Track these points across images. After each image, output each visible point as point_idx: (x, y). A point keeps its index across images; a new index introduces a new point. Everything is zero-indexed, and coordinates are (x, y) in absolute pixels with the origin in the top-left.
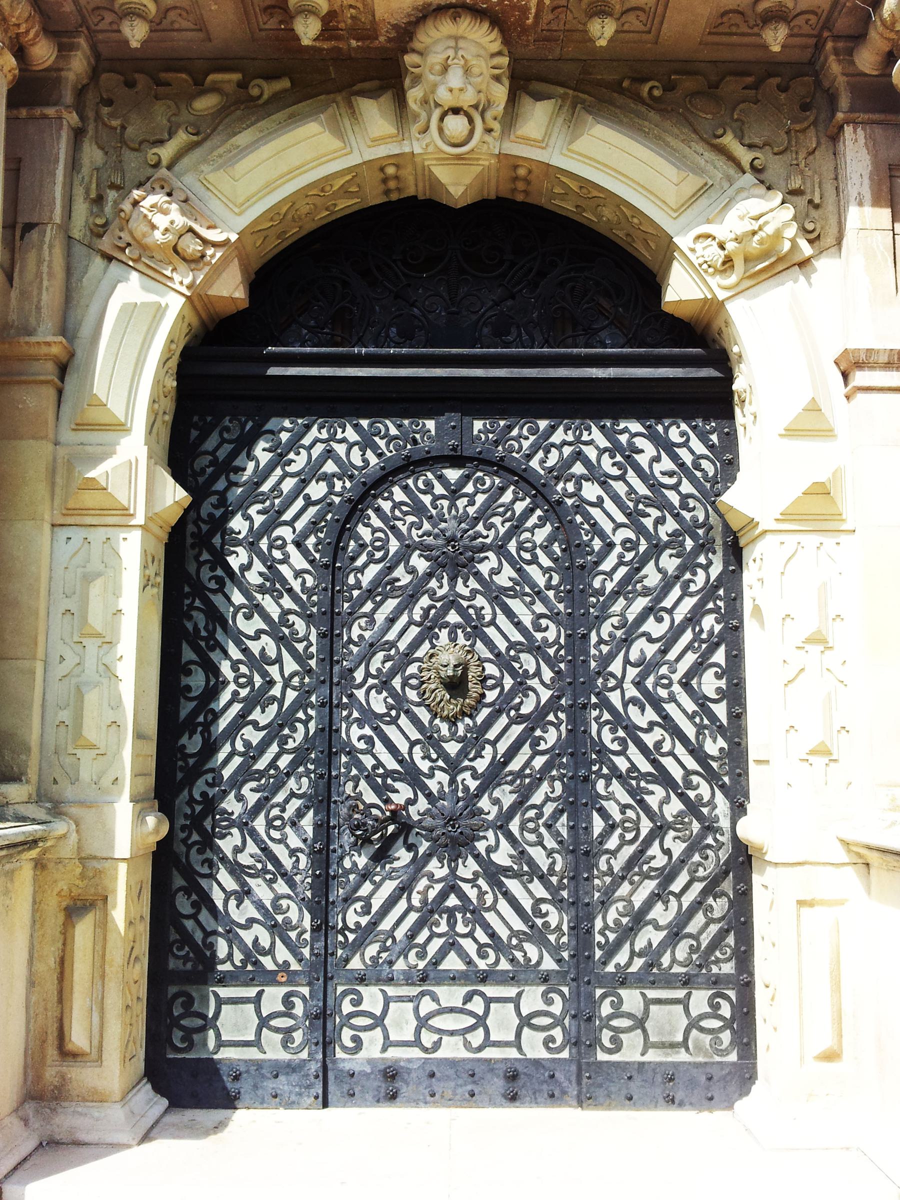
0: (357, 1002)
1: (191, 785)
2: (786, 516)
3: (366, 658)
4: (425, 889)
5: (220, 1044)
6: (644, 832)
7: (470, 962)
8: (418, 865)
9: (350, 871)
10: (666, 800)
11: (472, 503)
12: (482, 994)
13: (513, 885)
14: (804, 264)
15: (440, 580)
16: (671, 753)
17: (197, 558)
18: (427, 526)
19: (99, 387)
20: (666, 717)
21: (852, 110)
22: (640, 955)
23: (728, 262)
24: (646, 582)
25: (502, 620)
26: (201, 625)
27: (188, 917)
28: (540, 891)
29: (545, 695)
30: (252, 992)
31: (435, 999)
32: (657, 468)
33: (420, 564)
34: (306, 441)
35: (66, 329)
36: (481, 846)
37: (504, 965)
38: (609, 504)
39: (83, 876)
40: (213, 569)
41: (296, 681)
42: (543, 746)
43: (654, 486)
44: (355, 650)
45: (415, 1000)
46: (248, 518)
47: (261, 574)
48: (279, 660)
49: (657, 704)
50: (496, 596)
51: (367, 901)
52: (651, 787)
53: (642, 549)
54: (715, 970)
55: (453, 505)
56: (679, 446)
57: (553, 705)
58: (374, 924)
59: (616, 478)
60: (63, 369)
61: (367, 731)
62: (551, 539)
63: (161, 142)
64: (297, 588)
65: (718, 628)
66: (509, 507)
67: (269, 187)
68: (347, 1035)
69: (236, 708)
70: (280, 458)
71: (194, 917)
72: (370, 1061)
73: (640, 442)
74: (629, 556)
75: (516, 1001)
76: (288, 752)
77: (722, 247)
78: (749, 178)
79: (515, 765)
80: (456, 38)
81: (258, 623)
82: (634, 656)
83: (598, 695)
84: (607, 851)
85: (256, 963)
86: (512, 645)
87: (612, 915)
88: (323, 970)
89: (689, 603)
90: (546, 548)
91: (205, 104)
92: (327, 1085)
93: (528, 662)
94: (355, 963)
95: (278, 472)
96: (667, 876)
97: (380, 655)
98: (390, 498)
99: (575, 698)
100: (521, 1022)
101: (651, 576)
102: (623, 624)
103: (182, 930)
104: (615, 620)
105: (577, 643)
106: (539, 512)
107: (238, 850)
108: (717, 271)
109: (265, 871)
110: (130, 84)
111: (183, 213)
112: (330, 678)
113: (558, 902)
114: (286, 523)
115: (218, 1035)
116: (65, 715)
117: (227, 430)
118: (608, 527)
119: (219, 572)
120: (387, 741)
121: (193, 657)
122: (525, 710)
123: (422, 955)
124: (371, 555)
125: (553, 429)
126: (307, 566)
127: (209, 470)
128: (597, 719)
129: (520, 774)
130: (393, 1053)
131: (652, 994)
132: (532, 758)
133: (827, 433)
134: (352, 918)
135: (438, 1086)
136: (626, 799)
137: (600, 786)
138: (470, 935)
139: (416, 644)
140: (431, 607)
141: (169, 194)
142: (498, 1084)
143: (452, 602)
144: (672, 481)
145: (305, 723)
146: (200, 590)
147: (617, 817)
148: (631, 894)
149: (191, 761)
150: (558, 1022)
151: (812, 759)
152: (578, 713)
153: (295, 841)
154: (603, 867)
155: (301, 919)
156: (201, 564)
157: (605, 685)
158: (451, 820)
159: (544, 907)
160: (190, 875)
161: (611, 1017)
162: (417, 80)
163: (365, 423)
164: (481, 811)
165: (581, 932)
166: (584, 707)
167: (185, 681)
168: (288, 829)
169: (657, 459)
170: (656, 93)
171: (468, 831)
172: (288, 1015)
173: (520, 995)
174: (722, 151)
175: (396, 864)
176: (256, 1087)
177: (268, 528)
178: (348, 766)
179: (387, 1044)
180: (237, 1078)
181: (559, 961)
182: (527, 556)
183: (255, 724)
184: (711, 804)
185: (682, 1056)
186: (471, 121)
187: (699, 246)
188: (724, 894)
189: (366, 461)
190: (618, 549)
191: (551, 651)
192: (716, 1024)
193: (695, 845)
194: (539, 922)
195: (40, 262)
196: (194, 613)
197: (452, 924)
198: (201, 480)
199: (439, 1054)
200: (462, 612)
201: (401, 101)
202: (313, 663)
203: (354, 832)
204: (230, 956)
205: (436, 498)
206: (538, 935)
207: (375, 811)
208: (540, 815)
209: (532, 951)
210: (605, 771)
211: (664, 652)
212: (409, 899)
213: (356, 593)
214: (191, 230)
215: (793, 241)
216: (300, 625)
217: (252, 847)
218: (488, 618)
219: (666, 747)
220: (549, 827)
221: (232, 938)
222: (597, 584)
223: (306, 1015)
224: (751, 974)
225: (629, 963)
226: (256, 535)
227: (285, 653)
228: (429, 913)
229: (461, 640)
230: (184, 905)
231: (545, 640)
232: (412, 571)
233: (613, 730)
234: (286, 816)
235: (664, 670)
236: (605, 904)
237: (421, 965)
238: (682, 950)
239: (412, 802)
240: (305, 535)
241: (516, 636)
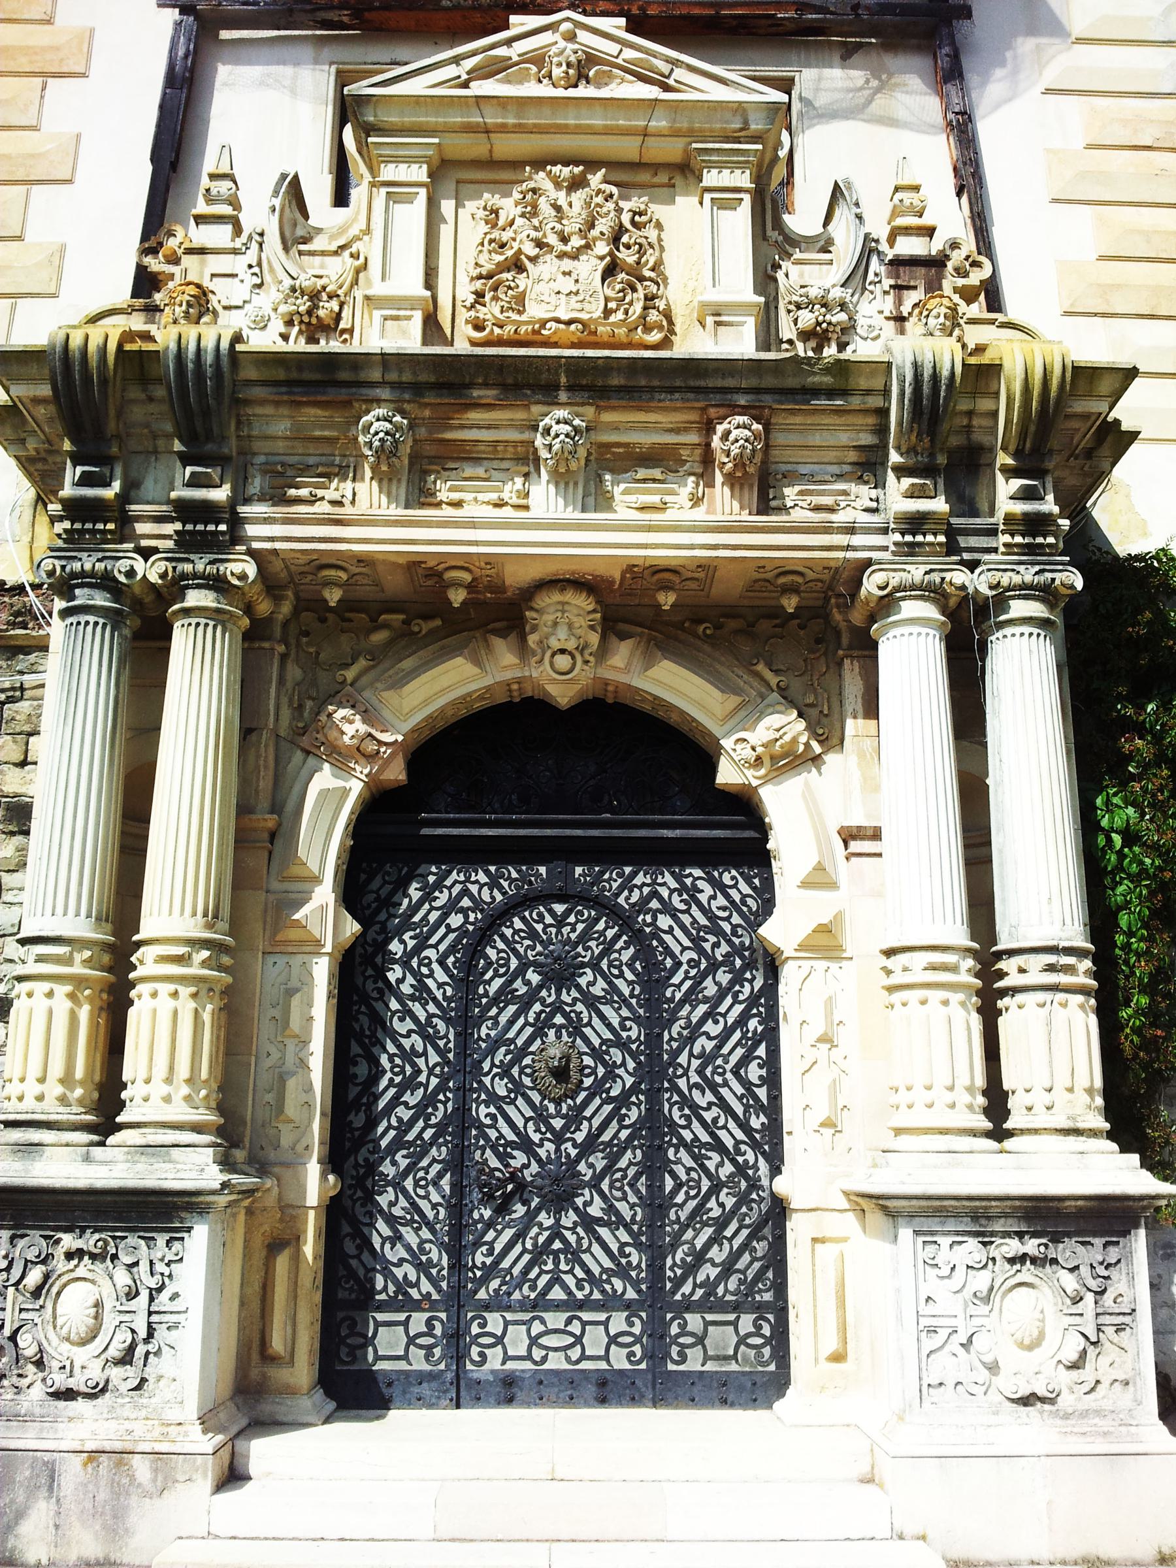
0: (483, 1325)
1: (357, 1151)
2: (802, 947)
3: (492, 1051)
4: (537, 1236)
5: (378, 1358)
6: (704, 1189)
7: (570, 1293)
8: (531, 1216)
9: (478, 1221)
10: (721, 1164)
11: (573, 930)
12: (579, 1319)
13: (604, 1232)
14: (816, 760)
16: (725, 1127)
17: (363, 973)
18: (539, 948)
19: (302, 852)
20: (721, 1098)
21: (850, 647)
22: (701, 1286)
23: (758, 758)
24: (706, 993)
25: (596, 1021)
26: (366, 1027)
27: (353, 1257)
28: (625, 1237)
29: (629, 1081)
30: (402, 1317)
31: (543, 1322)
32: (714, 904)
33: (534, 977)
34: (448, 883)
35: (276, 808)
36: (579, 1201)
37: (597, 1295)
38: (678, 932)
39: (281, 1220)
40: (375, 982)
41: (438, 1070)
42: (627, 1122)
43: (712, 918)
44: (484, 1045)
45: (528, 1323)
46: (402, 942)
48: (425, 1054)
49: (714, 1088)
50: (591, 1002)
51: (491, 1244)
52: (709, 1154)
53: (703, 967)
54: (758, 1298)
55: (559, 932)
56: (731, 887)
57: (635, 1089)
58: (496, 1263)
59: (682, 912)
60: (273, 835)
61: (492, 1110)
62: (633, 959)
63: (347, 666)
64: (440, 997)
65: (760, 1029)
66: (602, 933)
67: (426, 702)
68: (475, 1351)
69: (392, 1091)
70: (428, 897)
71: (358, 1257)
72: (493, 1372)
73: (701, 884)
74: (693, 972)
75: (606, 1323)
76: (432, 1126)
77: (754, 749)
78: (775, 696)
79: (606, 1137)
80: (563, 604)
81: (409, 1024)
82: (697, 1050)
83: (669, 1081)
84: (676, 1205)
85: (406, 1294)
86: (604, 1042)
87: (679, 1255)
88: (457, 1299)
89: (739, 1008)
90: (630, 966)
91: (379, 637)
92: (460, 1390)
93: (616, 1055)
94: (482, 1295)
95: (427, 906)
96: (721, 1224)
97: (503, 1050)
98: (511, 926)
99: (651, 1083)
100: (612, 1340)
101: (710, 989)
102: (689, 1024)
103: (348, 1267)
104: (682, 1022)
105: (653, 1041)
106: (625, 938)
107: (392, 1204)
108: (751, 766)
109: (413, 1221)
110: (323, 620)
111: (364, 721)
112: (463, 1069)
113: (638, 1245)
114: (431, 946)
115: (376, 1351)
116: (269, 1097)
117: (388, 874)
118: (677, 949)
119: (380, 984)
120: (508, 1118)
121: (360, 1051)
122: (614, 1093)
123: (533, 1288)
124: (496, 971)
125: (634, 874)
126: (447, 980)
127: (374, 905)
128: (668, 1100)
129: (609, 1144)
130: (510, 1365)
131: (710, 1317)
132: (618, 1131)
133: (832, 885)
134: (479, 1259)
135: (545, 1392)
136: (690, 1163)
137: (671, 1153)
138: (571, 1272)
139: (530, 1041)
140: (542, 1011)
141: (353, 707)
142: (591, 1390)
143: (558, 1007)
144: (725, 914)
145: (445, 1103)
146: (365, 999)
147: (684, 1178)
148: (694, 1238)
149: (357, 1133)
150: (638, 1340)
151: (822, 1130)
152: (654, 1097)
153: (435, 1198)
154: (673, 1217)
155: (440, 1259)
156: (366, 978)
157: (674, 1073)
158: (557, 1180)
159: (627, 1250)
160: (355, 1224)
161: (678, 1336)
162: (535, 629)
163: (492, 869)
164: (580, 1173)
165: (656, 1269)
166: (659, 1090)
167: (353, 1070)
168: (430, 1188)
169: (714, 897)
171: (569, 1189)
172: (429, 1334)
173: (608, 1318)
174: (757, 675)
175: (514, 1216)
176: (404, 1392)
177: (418, 950)
178: (477, 1138)
179: (506, 1358)
180: (390, 1385)
181: (639, 1292)
182: (616, 972)
183: (406, 1104)
184: (755, 1167)
185: (733, 1367)
186: (573, 657)
187: (739, 747)
188: (764, 1238)
190: (685, 967)
191: (634, 1047)
192: (758, 1341)
193: (743, 1199)
194: (624, 1261)
195: (258, 757)
196: (361, 1017)
197: (556, 1263)
198: (367, 912)
199: (545, 1366)
200: (566, 1015)
201: (523, 638)
202: (451, 1056)
203: (479, 1190)
204: (385, 1288)
205: (546, 926)
206: (622, 1272)
207: (497, 1174)
208: (624, 1177)
209: (618, 1284)
210: (675, 1141)
211: (719, 1047)
212: (523, 1243)
213: (484, 1001)
214: (370, 735)
215: (807, 745)
216: (441, 1026)
217: (403, 1202)
218: (585, 1020)
219: (721, 1122)
220: (631, 1185)
221: (388, 1275)
222: (668, 994)
223: (444, 1335)
224: (786, 1301)
225: (692, 1293)
226: (408, 955)
227: (429, 1048)
228: (539, 1254)
229: (565, 1038)
230: (350, 1247)
231: (629, 1037)
232: (527, 983)
233: (681, 1109)
234: (429, 1177)
235: (719, 1062)
236: (674, 1247)
237: (533, 1295)
238: (732, 1284)
239: (526, 1166)
241: (608, 1035)
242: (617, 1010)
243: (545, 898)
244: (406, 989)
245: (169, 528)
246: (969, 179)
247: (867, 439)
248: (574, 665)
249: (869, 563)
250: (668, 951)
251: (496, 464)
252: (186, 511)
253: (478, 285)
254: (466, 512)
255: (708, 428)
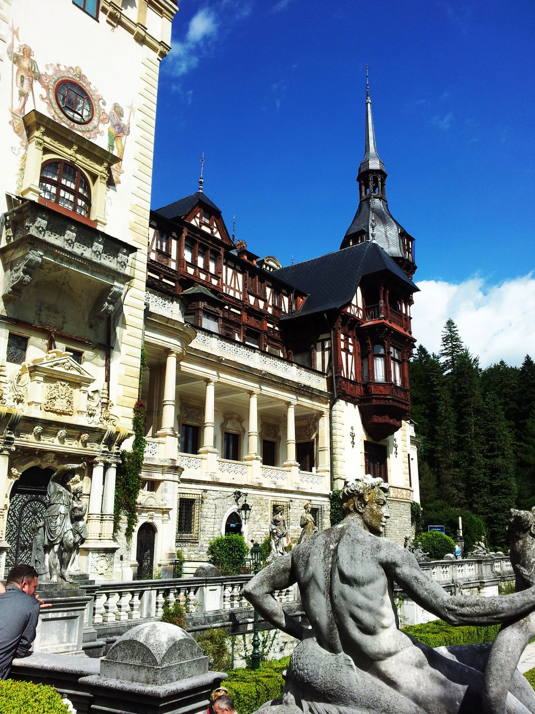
3: (24, 525)
143: (34, 519)
177: (14, 508)
243: (34, 500)
244: (12, 515)
245: (3, 440)
246: (107, 379)
247: (100, 438)
249: (96, 456)
252: (8, 438)
253: (48, 401)
255: (81, 434)
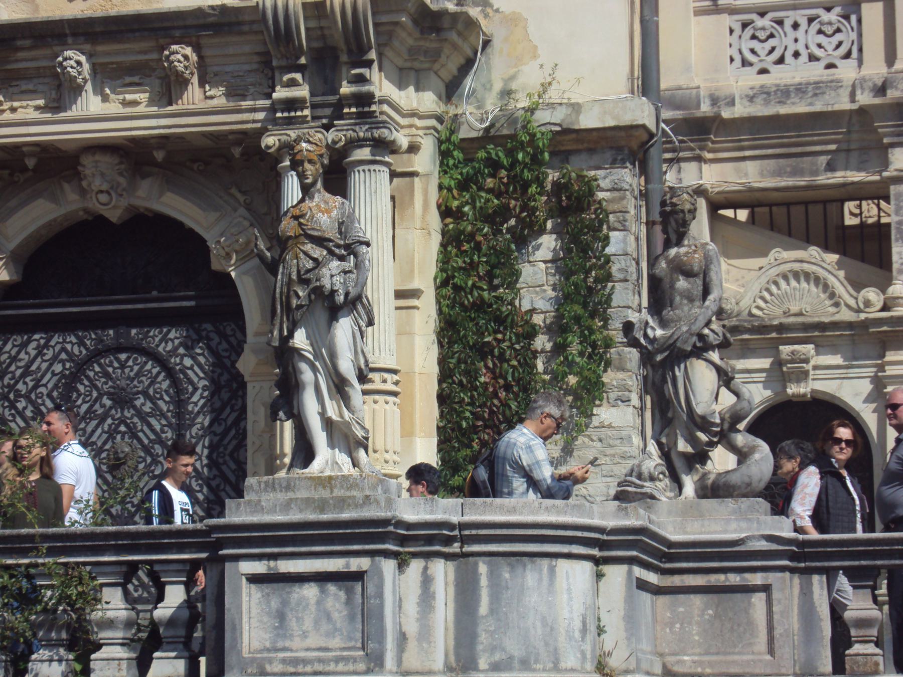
15: (116, 411)
16: (224, 490)
18: (110, 383)
25: (145, 428)
32: (220, 348)
33: (108, 402)
37: (145, 595)
38: (196, 368)
47: (32, 411)
56: (231, 336)
62: (170, 386)
73: (212, 335)
80: (97, 162)
86: (151, 441)
95: (39, 359)
118: (196, 379)
122: (157, 472)
125: (169, 332)
127: (8, 361)
139: (105, 443)
143: (123, 421)
144: (226, 354)
169: (220, 343)
170: (200, 168)
177: (36, 387)
189: (81, 352)
200: (127, 425)
211: (221, 440)
219: (222, 487)
229: (126, 439)
231: (166, 437)
232: (103, 406)
233: (196, 481)
235: (221, 449)
240: (52, 391)
241: (152, 437)
242: (159, 421)
244: (29, 413)
248: (111, 199)
250: (191, 382)
251: (41, 80)
254: (20, 115)
